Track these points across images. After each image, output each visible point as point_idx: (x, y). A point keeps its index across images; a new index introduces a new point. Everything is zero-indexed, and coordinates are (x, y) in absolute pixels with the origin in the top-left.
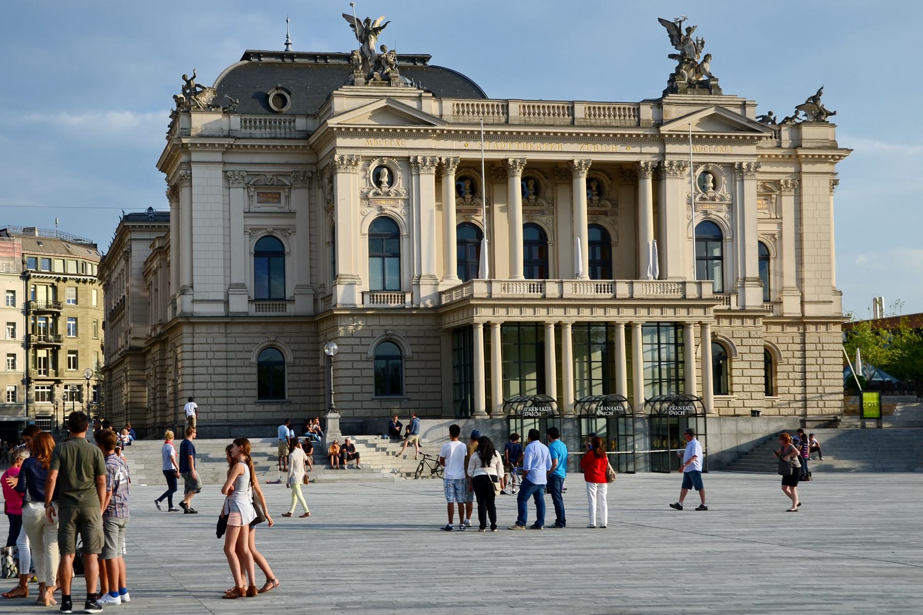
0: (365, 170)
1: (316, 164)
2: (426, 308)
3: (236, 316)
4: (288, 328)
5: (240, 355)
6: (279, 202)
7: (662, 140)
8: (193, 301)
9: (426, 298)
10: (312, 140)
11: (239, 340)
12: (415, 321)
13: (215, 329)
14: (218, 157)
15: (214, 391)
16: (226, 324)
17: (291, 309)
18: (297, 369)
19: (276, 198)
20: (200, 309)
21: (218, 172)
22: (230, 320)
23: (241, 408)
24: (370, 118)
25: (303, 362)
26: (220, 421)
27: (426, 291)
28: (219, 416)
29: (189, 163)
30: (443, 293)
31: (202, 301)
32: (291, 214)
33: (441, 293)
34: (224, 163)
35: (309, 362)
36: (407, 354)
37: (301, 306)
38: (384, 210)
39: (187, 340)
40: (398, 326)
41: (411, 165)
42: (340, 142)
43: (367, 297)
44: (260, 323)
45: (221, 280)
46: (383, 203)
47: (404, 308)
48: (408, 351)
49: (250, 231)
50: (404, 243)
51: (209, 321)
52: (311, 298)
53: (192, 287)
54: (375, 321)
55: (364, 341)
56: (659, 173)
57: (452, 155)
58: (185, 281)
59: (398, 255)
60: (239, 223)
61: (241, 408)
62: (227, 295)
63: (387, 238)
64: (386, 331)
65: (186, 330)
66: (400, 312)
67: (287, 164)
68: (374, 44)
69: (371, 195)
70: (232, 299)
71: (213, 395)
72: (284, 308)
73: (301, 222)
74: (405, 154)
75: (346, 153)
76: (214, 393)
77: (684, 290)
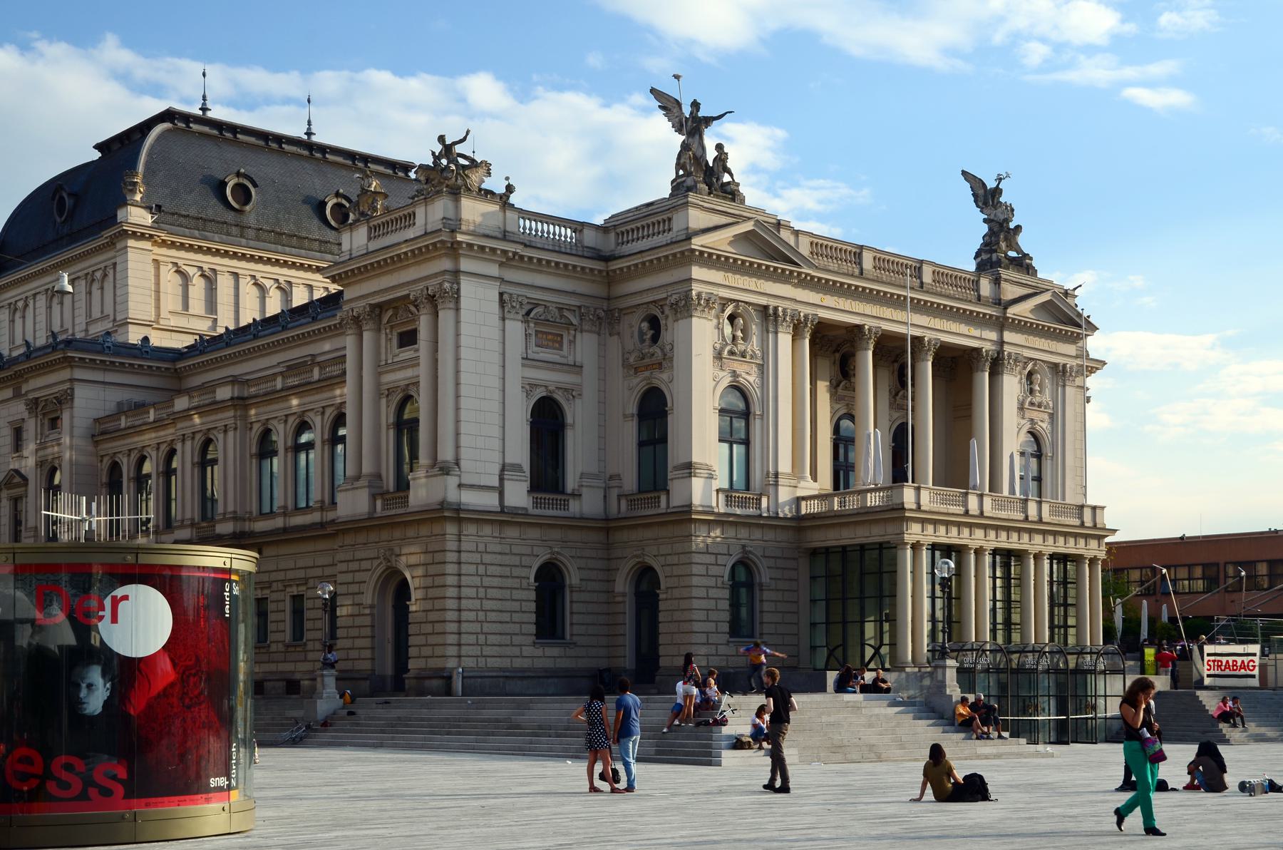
0: (718, 317)
1: (608, 299)
2: (785, 519)
3: (515, 512)
4: (573, 535)
5: (517, 572)
6: (561, 348)
8: (460, 486)
9: (785, 504)
10: (616, 265)
11: (516, 550)
12: (770, 535)
13: (487, 530)
15: (485, 625)
16: (502, 523)
17: (574, 507)
20: (471, 499)
22: (505, 518)
23: (516, 651)
24: (731, 243)
26: (493, 669)
27: (785, 495)
28: (493, 663)
30: (804, 498)
31: (472, 486)
36: (764, 580)
37: (589, 504)
38: (738, 376)
39: (451, 545)
40: (755, 540)
42: (697, 272)
44: (561, 526)
45: (497, 458)
46: (741, 368)
47: (760, 516)
49: (530, 387)
50: (756, 426)
51: (481, 518)
53: (457, 464)
54: (731, 532)
55: (721, 560)
57: (809, 310)
58: (446, 454)
59: (746, 442)
60: (516, 373)
61: (516, 651)
62: (501, 479)
63: (741, 417)
64: (744, 546)
65: (451, 529)
67: (573, 293)
69: (725, 353)
70: (508, 485)
71: (485, 630)
72: (565, 506)
74: (763, 301)
76: (486, 628)
77: (1081, 516)
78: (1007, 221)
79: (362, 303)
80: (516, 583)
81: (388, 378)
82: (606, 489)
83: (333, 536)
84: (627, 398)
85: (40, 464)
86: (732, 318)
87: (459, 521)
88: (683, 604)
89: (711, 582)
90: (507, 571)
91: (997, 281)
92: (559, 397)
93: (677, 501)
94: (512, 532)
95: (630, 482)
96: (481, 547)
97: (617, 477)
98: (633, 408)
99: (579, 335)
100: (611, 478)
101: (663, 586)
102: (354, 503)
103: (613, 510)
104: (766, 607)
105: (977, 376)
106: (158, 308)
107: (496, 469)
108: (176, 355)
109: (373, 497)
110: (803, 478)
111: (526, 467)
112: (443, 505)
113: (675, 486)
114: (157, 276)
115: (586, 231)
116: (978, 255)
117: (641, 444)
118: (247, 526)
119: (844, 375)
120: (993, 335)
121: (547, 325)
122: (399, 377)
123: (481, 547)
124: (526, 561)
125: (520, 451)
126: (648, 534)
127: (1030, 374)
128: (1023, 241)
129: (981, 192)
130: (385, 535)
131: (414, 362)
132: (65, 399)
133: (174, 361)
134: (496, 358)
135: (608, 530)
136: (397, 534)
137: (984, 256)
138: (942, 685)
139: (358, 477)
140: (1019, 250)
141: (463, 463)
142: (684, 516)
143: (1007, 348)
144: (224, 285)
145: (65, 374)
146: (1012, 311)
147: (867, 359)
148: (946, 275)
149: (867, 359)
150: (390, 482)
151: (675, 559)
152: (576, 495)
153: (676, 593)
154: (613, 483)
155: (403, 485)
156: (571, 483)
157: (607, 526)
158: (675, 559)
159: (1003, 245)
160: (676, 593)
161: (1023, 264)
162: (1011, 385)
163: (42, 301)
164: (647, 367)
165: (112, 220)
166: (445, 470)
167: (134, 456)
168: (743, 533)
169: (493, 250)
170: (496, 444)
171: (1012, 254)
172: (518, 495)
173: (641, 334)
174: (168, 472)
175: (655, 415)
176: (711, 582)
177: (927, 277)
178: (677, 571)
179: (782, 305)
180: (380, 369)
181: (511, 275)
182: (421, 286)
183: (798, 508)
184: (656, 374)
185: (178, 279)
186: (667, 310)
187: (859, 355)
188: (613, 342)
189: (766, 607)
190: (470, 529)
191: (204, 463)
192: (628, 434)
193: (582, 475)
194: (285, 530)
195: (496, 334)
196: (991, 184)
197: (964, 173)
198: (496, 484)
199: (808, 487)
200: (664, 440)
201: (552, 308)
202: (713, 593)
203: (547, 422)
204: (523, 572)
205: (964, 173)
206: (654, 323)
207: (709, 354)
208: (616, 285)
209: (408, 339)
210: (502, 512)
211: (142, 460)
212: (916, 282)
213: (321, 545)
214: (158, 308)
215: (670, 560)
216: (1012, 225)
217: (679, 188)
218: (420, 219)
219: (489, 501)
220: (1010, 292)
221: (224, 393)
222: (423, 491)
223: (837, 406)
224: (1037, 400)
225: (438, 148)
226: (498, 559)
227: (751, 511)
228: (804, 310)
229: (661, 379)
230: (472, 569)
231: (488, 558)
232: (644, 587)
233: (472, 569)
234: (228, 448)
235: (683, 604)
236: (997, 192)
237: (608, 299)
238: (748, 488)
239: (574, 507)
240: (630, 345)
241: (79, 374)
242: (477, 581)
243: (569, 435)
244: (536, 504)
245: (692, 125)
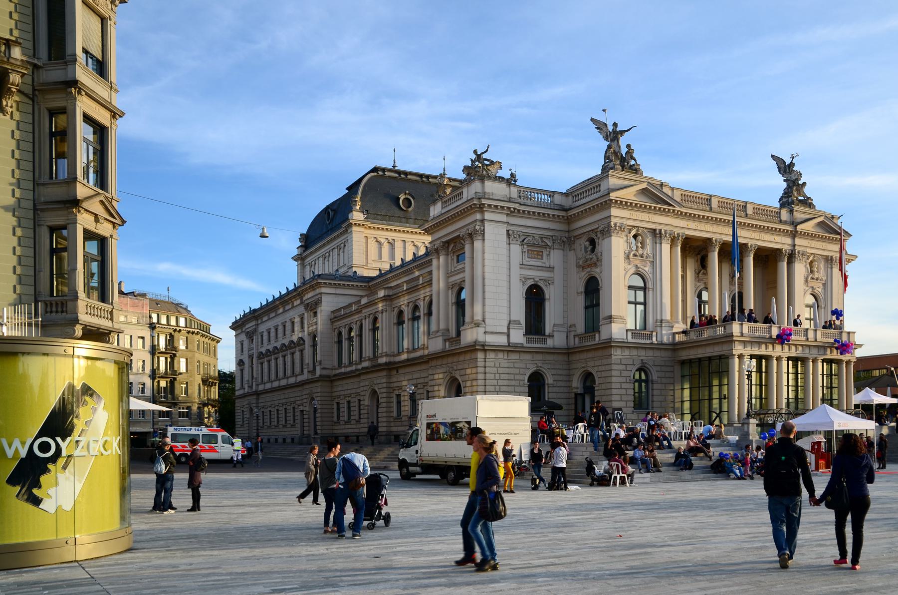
3: (516, 346)
4: (550, 357)
5: (517, 377)
7: (794, 235)
11: (516, 365)
13: (501, 355)
14: (503, 218)
17: (550, 343)
18: (555, 389)
19: (540, 255)
20: (491, 339)
21: (503, 230)
22: (510, 349)
25: (559, 384)
29: (483, 221)
31: (492, 333)
32: (551, 269)
33: (674, 334)
34: (508, 223)
35: (563, 384)
37: (558, 341)
39: (480, 363)
41: (656, 234)
43: (630, 334)
47: (652, 343)
48: (655, 376)
49: (524, 279)
51: (497, 349)
52: (565, 335)
54: (634, 352)
55: (629, 367)
56: (791, 258)
59: (644, 304)
60: (516, 272)
62: (509, 329)
65: (480, 355)
66: (651, 347)
68: (623, 141)
72: (545, 342)
73: (558, 275)
75: (619, 221)
78: (797, 179)
79: (439, 242)
80: (517, 383)
81: (452, 279)
82: (568, 332)
83: (427, 362)
84: (578, 283)
85: (309, 334)
86: (635, 237)
87: (485, 351)
88: (608, 392)
89: (624, 380)
90: (512, 377)
91: (791, 211)
92: (541, 284)
93: (604, 336)
94: (514, 356)
95: (581, 329)
96: (497, 365)
97: (574, 326)
98: (582, 289)
99: (552, 251)
100: (571, 326)
101: (597, 383)
102: (437, 345)
103: (572, 344)
104: (655, 392)
105: (780, 264)
106: (367, 259)
107: (506, 323)
108: (372, 279)
109: (445, 341)
110: (678, 322)
111: (523, 322)
112: (476, 343)
113: (603, 329)
114: (367, 243)
115: (555, 196)
116: (781, 199)
117: (586, 308)
118: (392, 359)
119: (703, 264)
120: (788, 241)
121: (535, 246)
122: (457, 278)
123: (497, 365)
124: (522, 371)
125: (519, 313)
126: (590, 355)
127: (811, 262)
128: (807, 191)
129: (782, 166)
130: (450, 360)
131: (463, 270)
132: (318, 303)
133: (368, 282)
134: (506, 265)
135: (568, 354)
136: (455, 359)
137: (784, 200)
138: (747, 434)
139: (437, 332)
140: (805, 196)
141: (487, 321)
142: (609, 344)
143: (797, 248)
144: (399, 246)
145: (318, 291)
146: (799, 228)
147: (714, 257)
148: (761, 211)
149: (714, 257)
150: (453, 333)
151: (603, 368)
152: (551, 336)
153: (604, 386)
154: (573, 329)
155: (459, 334)
156: (548, 330)
157: (568, 352)
158: (603, 368)
159: (795, 193)
160: (604, 386)
161: (807, 202)
162: (800, 269)
163: (321, 259)
164: (589, 266)
165: (347, 219)
166: (477, 325)
167: (347, 327)
168: (642, 353)
169: (502, 207)
170: (506, 310)
171: (801, 198)
172: (518, 336)
173: (586, 248)
174: (360, 336)
175: (593, 291)
176: (624, 380)
177: (750, 211)
178: (604, 374)
179: (664, 228)
180: (448, 275)
181: (513, 220)
182: (465, 229)
183: (674, 338)
184: (594, 269)
185: (376, 245)
186: (599, 235)
187: (710, 255)
188: (571, 254)
189: (655, 392)
190: (491, 355)
191: (375, 329)
192: (580, 302)
193: (554, 325)
194: (408, 360)
195: (505, 252)
196: (788, 162)
197: (772, 156)
198: (506, 331)
199: (680, 327)
200: (598, 305)
201: (537, 237)
202: (624, 386)
203: (535, 298)
204: (521, 377)
205: (772, 156)
206: (592, 242)
207: (622, 257)
208: (573, 225)
209: (460, 258)
210: (509, 346)
211: (351, 330)
212: (743, 214)
213: (423, 367)
214: (367, 259)
215: (600, 368)
216: (800, 182)
217: (605, 169)
218: (465, 196)
219: (502, 340)
220: (799, 216)
221: (381, 293)
222: (470, 336)
223: (698, 284)
224: (816, 275)
225: (474, 157)
226: (507, 370)
227: (648, 342)
228: (677, 231)
229: (596, 272)
230: (492, 376)
231: (501, 371)
232: (588, 384)
233: (492, 376)
234: (384, 321)
235: (608, 392)
236: (792, 164)
237: (568, 231)
238: (645, 329)
239: (550, 343)
240: (580, 256)
241: (324, 290)
242: (495, 382)
243: (547, 304)
244: (528, 341)
245: (613, 135)
